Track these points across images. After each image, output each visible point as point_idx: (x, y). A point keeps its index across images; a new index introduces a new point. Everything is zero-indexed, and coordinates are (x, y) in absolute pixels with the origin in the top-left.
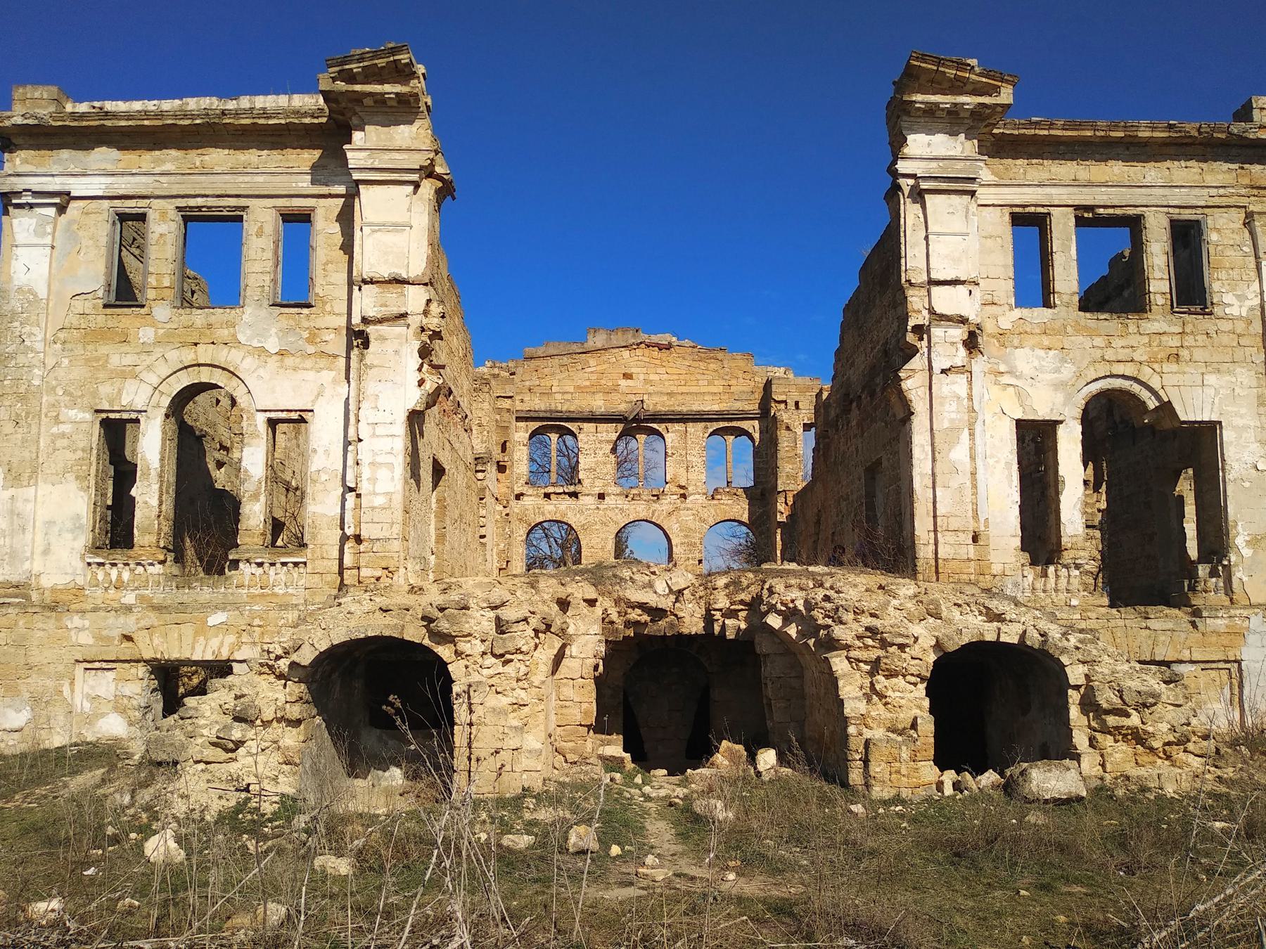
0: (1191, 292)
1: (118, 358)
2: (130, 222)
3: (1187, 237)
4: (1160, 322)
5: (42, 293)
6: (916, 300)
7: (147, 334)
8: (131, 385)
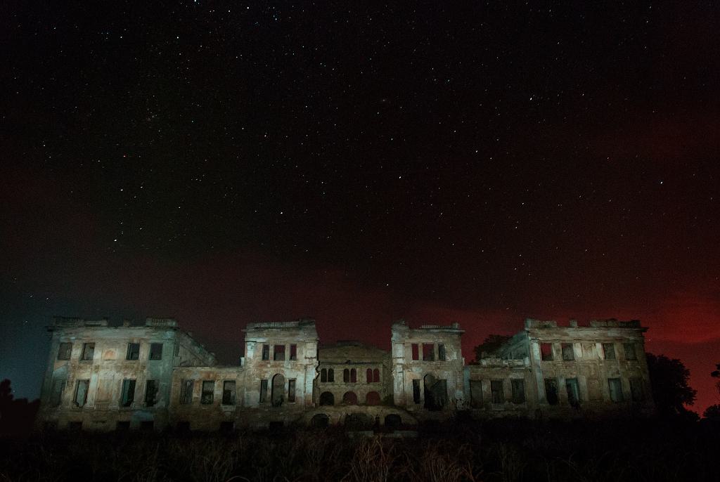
0: (442, 358)
1: (265, 370)
2: (266, 348)
3: (441, 347)
4: (436, 362)
5: (252, 358)
6: (394, 361)
7: (269, 366)
8: (267, 374)
